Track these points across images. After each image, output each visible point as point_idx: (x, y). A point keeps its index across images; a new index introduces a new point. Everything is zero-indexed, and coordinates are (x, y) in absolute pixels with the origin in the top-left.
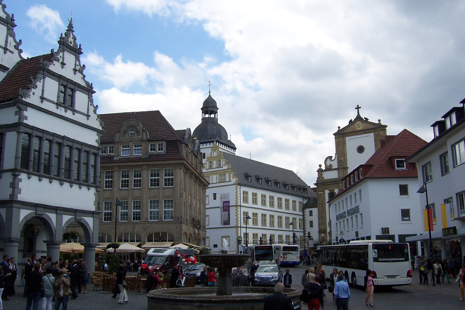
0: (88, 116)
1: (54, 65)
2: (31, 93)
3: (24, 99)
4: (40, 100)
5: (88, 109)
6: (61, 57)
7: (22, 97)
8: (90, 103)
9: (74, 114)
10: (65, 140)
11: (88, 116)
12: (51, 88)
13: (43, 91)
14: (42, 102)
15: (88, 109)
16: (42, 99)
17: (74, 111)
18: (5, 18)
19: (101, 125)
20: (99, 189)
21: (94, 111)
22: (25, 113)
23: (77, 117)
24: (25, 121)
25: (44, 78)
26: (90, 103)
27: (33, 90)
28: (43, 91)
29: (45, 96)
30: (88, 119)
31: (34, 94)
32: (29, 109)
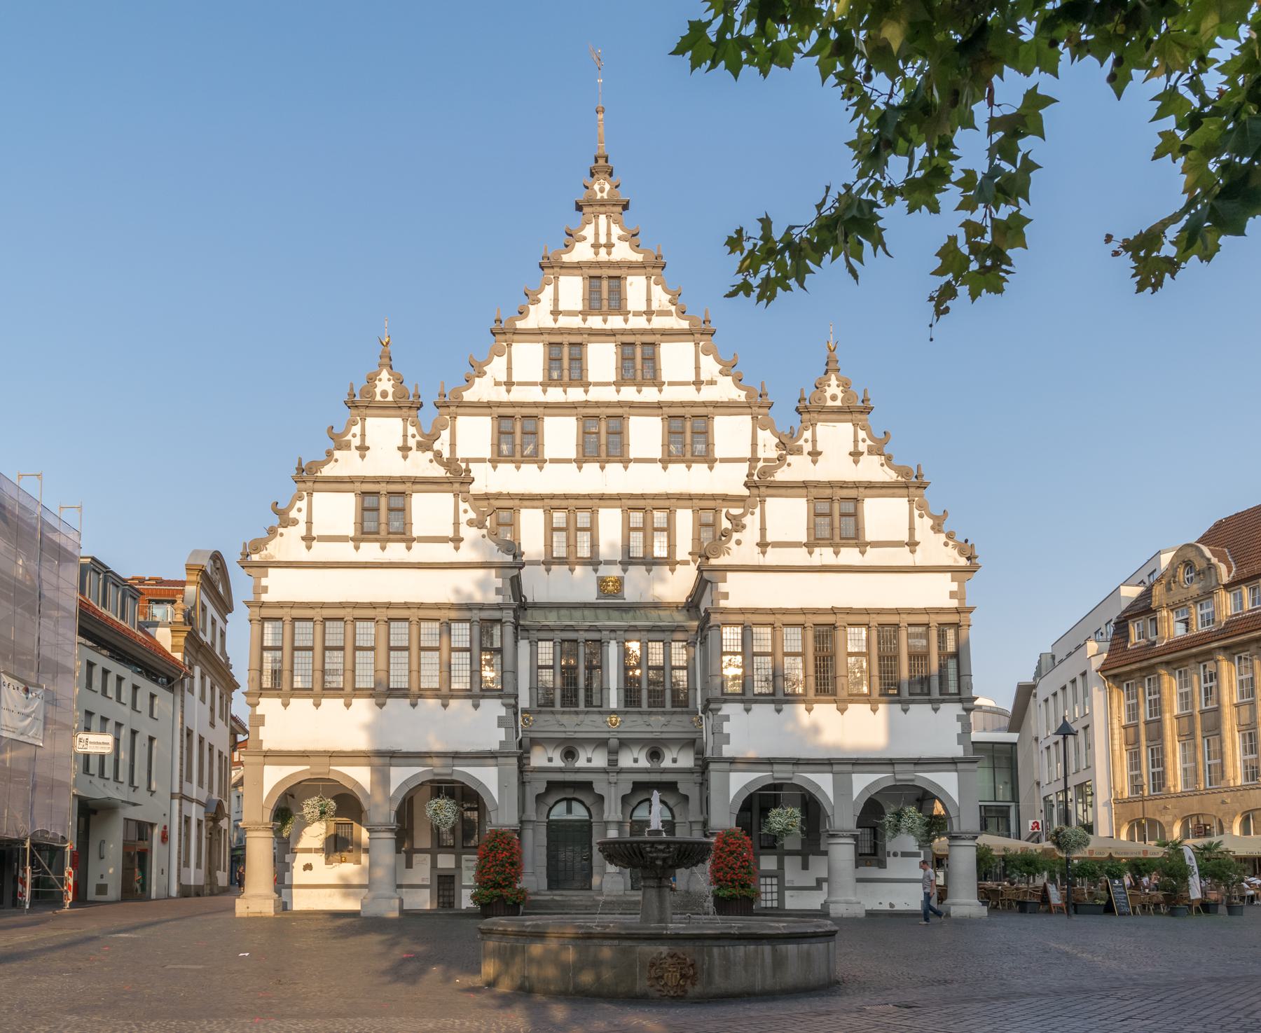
0: (912, 544)
1: (789, 465)
2: (732, 544)
3: (713, 562)
4: (758, 550)
5: (912, 529)
6: (806, 441)
7: (708, 558)
8: (916, 512)
9: (863, 553)
10: (839, 616)
11: (912, 544)
12: (788, 517)
13: (763, 529)
14: (764, 553)
15: (912, 529)
16: (763, 545)
17: (863, 546)
18: (743, 399)
19: (961, 553)
20: (968, 705)
21: (933, 528)
22: (723, 587)
23: (873, 557)
24: (723, 603)
25: (763, 502)
26: (916, 512)
27: (736, 536)
28: (763, 529)
29: (770, 538)
30: (913, 552)
31: (738, 542)
32: (729, 575)
